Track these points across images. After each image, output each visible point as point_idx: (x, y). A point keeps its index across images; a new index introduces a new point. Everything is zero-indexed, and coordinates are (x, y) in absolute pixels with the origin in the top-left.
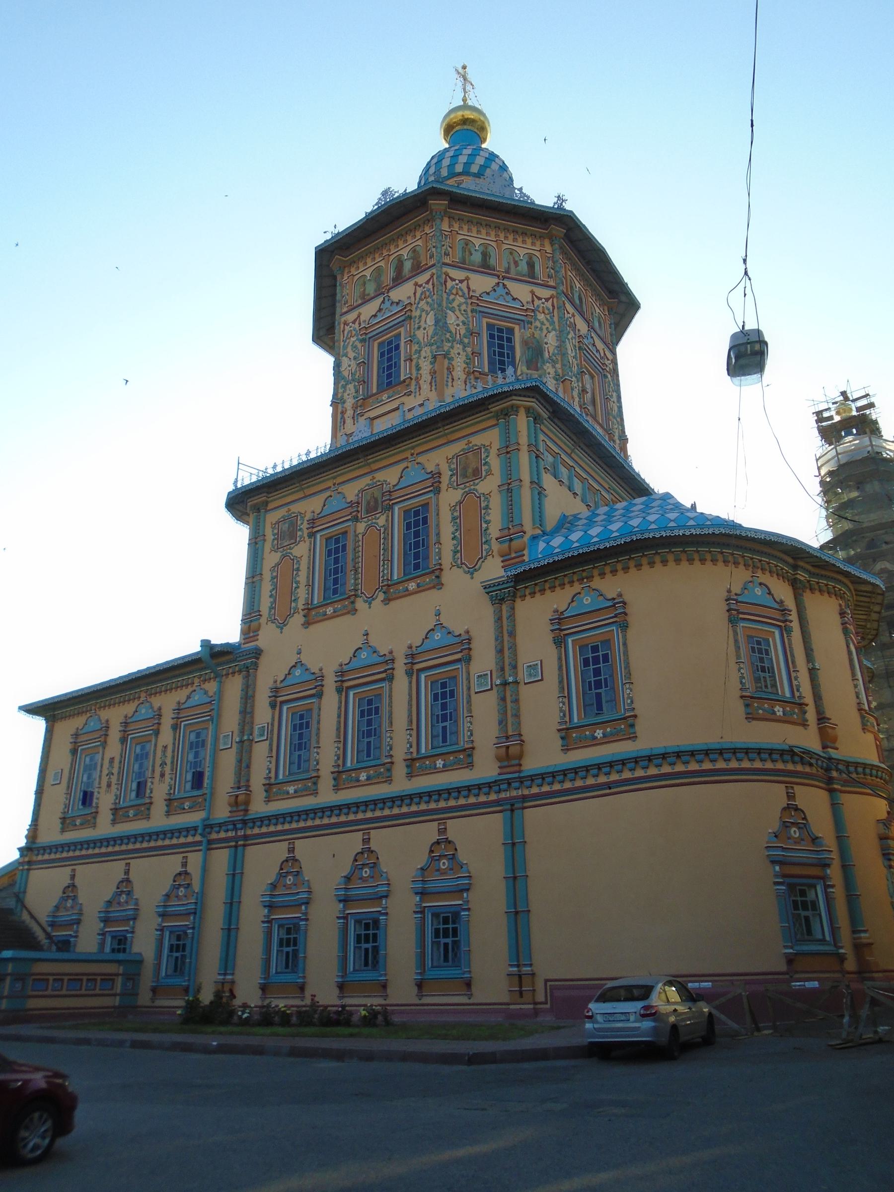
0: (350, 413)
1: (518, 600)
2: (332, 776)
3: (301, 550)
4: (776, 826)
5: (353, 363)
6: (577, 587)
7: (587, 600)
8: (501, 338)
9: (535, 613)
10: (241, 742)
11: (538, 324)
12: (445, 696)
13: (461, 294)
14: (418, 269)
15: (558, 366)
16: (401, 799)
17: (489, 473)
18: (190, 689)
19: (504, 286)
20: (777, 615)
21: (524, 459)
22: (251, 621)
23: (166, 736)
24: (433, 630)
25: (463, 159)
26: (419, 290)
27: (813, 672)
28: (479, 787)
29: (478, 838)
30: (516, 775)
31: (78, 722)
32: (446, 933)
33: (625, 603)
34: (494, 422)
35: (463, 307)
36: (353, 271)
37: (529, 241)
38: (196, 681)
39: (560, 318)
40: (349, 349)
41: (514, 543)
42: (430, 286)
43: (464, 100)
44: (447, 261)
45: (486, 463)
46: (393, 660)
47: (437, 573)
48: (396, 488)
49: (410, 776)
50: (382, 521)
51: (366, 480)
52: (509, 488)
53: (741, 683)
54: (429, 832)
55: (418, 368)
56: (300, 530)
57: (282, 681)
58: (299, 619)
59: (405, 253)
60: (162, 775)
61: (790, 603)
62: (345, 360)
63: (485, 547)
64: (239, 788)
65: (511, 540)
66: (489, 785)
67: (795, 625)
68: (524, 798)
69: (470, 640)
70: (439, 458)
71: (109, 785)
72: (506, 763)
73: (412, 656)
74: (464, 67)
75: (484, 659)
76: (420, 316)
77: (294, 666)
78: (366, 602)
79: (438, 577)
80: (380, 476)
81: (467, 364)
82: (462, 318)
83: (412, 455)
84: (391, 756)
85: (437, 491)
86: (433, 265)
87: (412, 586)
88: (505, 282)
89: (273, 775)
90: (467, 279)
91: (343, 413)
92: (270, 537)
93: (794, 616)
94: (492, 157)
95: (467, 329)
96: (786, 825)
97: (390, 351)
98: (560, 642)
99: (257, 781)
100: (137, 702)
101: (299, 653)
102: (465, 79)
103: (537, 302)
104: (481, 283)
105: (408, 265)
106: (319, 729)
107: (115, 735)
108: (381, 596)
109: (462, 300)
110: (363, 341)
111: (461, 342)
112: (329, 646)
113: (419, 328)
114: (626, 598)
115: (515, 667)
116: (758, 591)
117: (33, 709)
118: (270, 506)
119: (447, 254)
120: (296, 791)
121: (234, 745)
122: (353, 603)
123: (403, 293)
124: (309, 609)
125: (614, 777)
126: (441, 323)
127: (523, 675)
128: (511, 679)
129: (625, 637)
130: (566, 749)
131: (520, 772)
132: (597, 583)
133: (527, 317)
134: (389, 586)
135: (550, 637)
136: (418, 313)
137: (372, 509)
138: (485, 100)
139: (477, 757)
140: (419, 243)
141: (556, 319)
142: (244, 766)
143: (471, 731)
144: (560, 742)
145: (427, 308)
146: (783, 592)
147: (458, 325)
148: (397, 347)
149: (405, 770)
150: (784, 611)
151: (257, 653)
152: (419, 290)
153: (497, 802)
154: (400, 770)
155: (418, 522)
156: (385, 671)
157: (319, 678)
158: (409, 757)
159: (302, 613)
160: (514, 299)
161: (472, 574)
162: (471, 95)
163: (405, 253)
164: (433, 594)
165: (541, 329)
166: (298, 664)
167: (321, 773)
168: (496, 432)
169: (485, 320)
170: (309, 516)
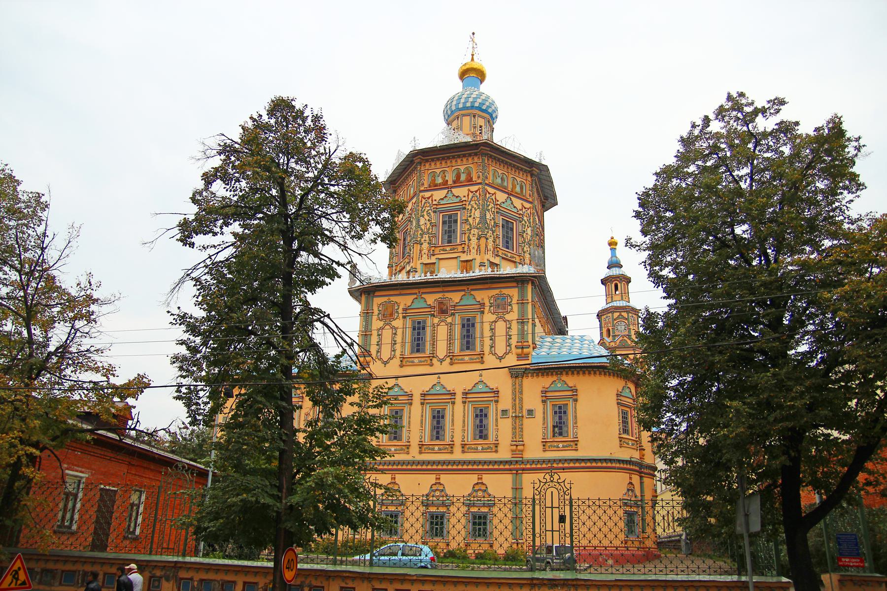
0: (425, 251)
3: (398, 323)
4: (626, 491)
5: (428, 223)
6: (555, 378)
7: (559, 385)
8: (507, 228)
9: (533, 388)
14: (470, 181)
16: (459, 462)
20: (631, 401)
26: (471, 195)
28: (501, 462)
29: (499, 485)
32: (479, 524)
34: (514, 284)
40: (425, 213)
42: (478, 194)
45: (510, 305)
49: (463, 452)
51: (440, 295)
54: (474, 478)
59: (462, 168)
66: (507, 462)
68: (523, 469)
70: (484, 296)
73: (465, 394)
74: (473, 34)
75: (506, 402)
80: (448, 295)
85: (483, 312)
86: (480, 183)
91: (421, 251)
92: (376, 312)
96: (628, 490)
97: (450, 222)
98: (544, 402)
104: (501, 197)
105: (463, 177)
108: (448, 360)
115: (521, 408)
116: (628, 391)
123: (461, 192)
124: (403, 359)
125: (566, 465)
126: (483, 217)
132: (564, 378)
135: (539, 399)
137: (443, 311)
139: (499, 448)
145: (475, 206)
148: (456, 221)
149: (461, 449)
152: (471, 195)
153: (510, 470)
154: (458, 449)
155: (468, 326)
163: (462, 168)
167: (411, 443)
168: (517, 289)
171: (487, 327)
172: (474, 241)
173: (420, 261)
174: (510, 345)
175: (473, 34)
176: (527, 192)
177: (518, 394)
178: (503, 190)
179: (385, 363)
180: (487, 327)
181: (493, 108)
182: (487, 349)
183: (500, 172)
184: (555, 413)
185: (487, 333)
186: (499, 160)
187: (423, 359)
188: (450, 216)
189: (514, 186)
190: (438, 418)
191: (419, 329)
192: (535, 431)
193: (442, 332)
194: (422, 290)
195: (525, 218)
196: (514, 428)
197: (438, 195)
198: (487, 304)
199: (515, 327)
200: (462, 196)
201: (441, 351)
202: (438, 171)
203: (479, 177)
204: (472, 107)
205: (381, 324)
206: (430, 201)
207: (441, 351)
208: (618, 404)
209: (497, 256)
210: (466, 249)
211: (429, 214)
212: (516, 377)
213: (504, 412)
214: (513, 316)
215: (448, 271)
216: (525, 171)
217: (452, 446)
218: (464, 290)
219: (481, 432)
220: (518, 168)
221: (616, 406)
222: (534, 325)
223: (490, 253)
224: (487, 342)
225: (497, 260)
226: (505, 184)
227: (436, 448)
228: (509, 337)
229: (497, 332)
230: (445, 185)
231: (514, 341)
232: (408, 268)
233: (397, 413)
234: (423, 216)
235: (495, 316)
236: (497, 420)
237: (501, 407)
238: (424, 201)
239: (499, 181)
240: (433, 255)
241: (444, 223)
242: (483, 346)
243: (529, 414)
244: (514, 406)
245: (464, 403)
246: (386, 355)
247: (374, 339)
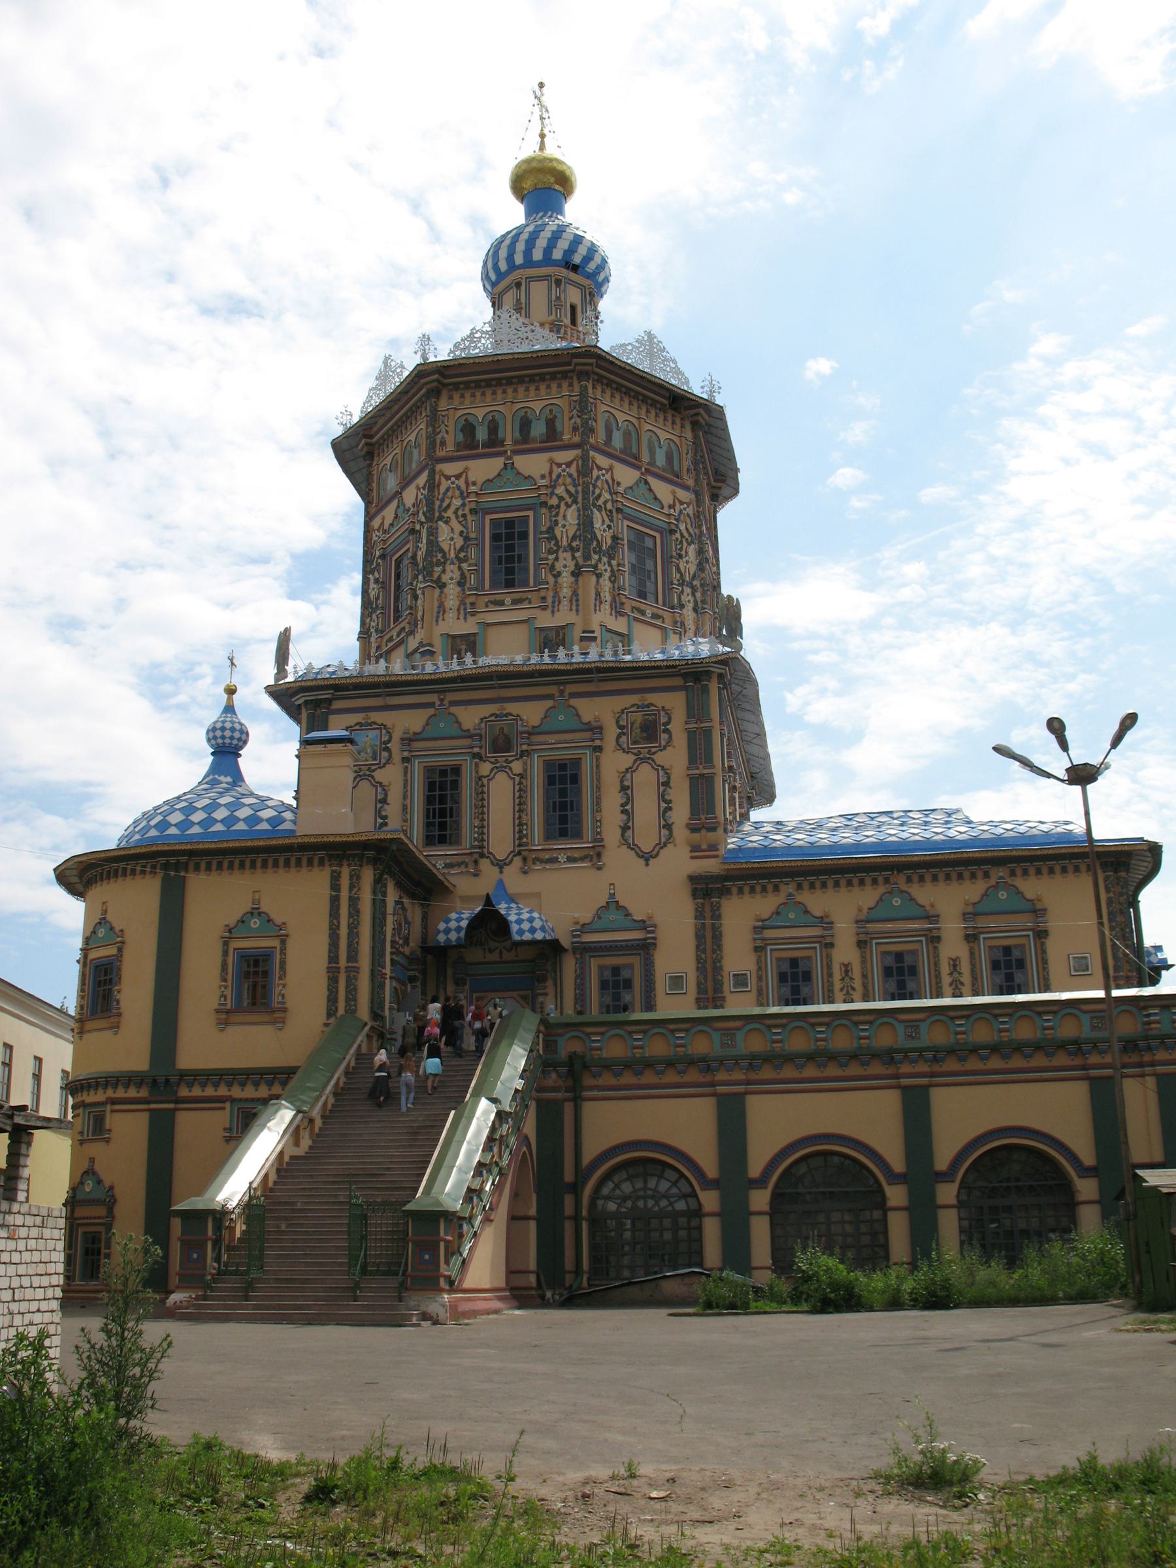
0: (452, 601)
13: (606, 487)
19: (646, 482)
25: (541, 243)
42: (573, 470)
47: (598, 849)
48: (537, 730)
51: (493, 708)
63: (664, 832)
70: (601, 710)
76: (558, 506)
80: (511, 708)
81: (613, 582)
82: (607, 522)
83: (562, 693)
88: (650, 479)
97: (510, 536)
104: (626, 476)
105: (538, 429)
109: (609, 497)
118: (337, 705)
123: (533, 465)
147: (604, 531)
148: (524, 535)
152: (557, 471)
155: (564, 782)
165: (681, 543)
169: (626, 523)
172: (566, 579)
174: (669, 827)
178: (630, 458)
185: (612, 800)
188: (510, 523)
193: (501, 792)
195: (682, 527)
198: (611, 732)
200: (536, 474)
201: (501, 841)
207: (501, 841)
209: (622, 614)
210: (550, 600)
215: (507, 651)
223: (606, 607)
225: (620, 625)
228: (666, 807)
232: (413, 643)
238: (445, 484)
240: (473, 614)
241: (495, 538)
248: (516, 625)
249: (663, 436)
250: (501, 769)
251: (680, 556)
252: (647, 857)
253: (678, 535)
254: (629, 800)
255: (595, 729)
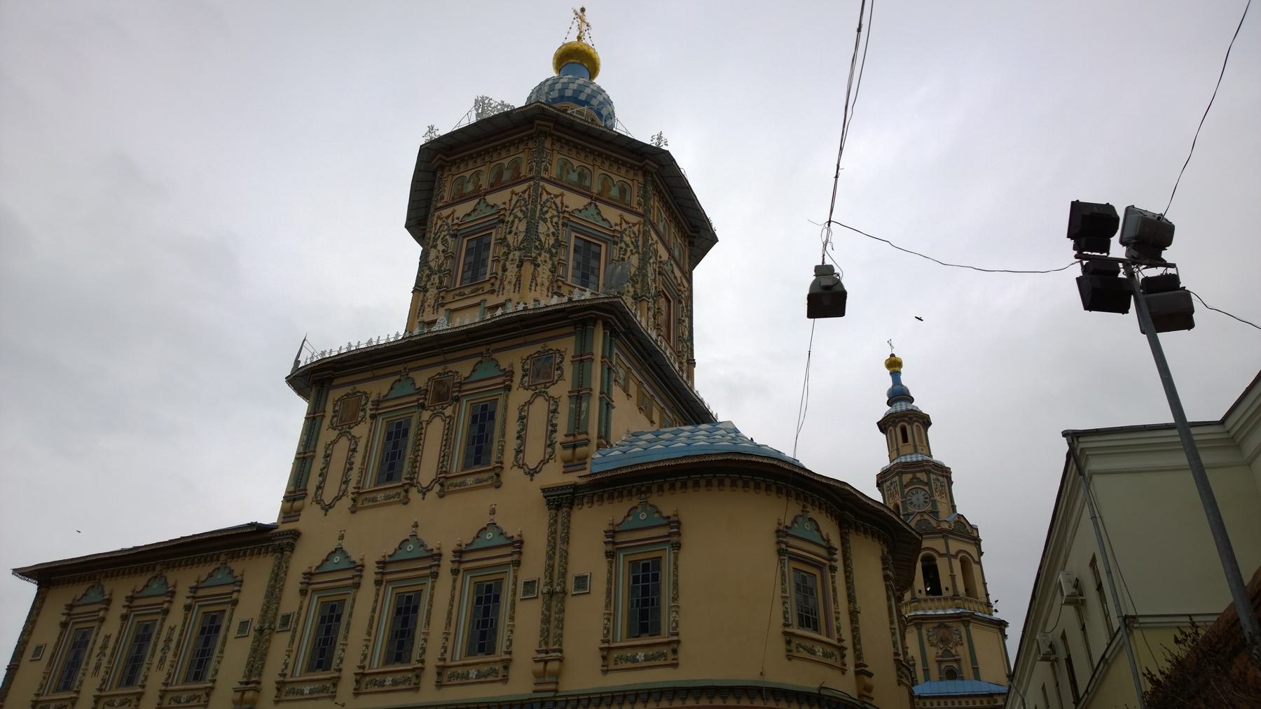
0: (431, 301)
1: (575, 508)
2: (354, 677)
3: (361, 431)
6: (635, 501)
7: (643, 516)
9: (590, 526)
10: (261, 631)
11: (623, 245)
12: (487, 600)
14: (517, 180)
15: (639, 286)
17: (561, 377)
18: (214, 566)
20: (823, 552)
21: (597, 369)
22: (295, 500)
23: (176, 617)
24: (485, 529)
27: (854, 614)
30: (552, 694)
31: (77, 591)
33: (679, 523)
34: (571, 329)
35: (555, 220)
36: (454, 170)
37: (623, 170)
38: (223, 558)
39: (645, 241)
40: (439, 242)
41: (578, 450)
42: (526, 196)
43: (579, 38)
44: (546, 176)
46: (440, 555)
49: (439, 685)
50: (448, 411)
51: (439, 369)
52: (579, 395)
53: (785, 618)
55: (504, 270)
56: (363, 410)
57: (318, 568)
58: (346, 502)
60: (162, 661)
61: (836, 542)
62: (433, 253)
63: (549, 450)
64: (247, 683)
65: (575, 447)
67: (839, 564)
69: (522, 542)
70: (514, 359)
71: (97, 667)
72: (541, 680)
73: (459, 553)
74: (583, 10)
75: (534, 566)
77: (334, 552)
78: (419, 492)
79: (498, 475)
80: (452, 367)
82: (552, 230)
84: (422, 661)
85: (509, 388)
86: (532, 178)
87: (470, 481)
89: (288, 672)
90: (562, 195)
91: (423, 302)
93: (839, 556)
94: (600, 91)
95: (557, 240)
98: (610, 555)
99: (270, 679)
100: (149, 575)
101: (342, 538)
102: (583, 21)
103: (624, 225)
104: (574, 201)
105: (507, 176)
106: (349, 624)
107: (117, 609)
108: (437, 488)
110: (454, 236)
111: (549, 251)
112: (374, 534)
113: (510, 232)
114: (683, 521)
115: (563, 575)
117: (25, 573)
118: (336, 382)
119: (546, 170)
120: (311, 692)
121: (252, 633)
122: (406, 491)
123: (499, 198)
124: (358, 493)
126: (531, 230)
127: (570, 585)
128: (558, 589)
129: (676, 558)
130: (605, 672)
131: (556, 691)
132: (654, 499)
133: (614, 238)
134: (447, 478)
136: (511, 218)
138: (598, 43)
139: (513, 673)
140: (521, 155)
141: (640, 243)
142: (258, 657)
143: (511, 641)
144: (600, 662)
145: (520, 215)
146: (829, 529)
150: (831, 550)
151: (296, 535)
152: (515, 198)
154: (429, 677)
155: (483, 420)
156: (431, 567)
157: (359, 568)
158: (442, 663)
159: (351, 496)
160: (604, 220)
161: (532, 475)
162: (587, 36)
163: (506, 162)
164: (492, 492)
166: (339, 550)
169: (573, 234)
170: (373, 397)
171: (513, 415)
172: (512, 269)
173: (421, 319)
175: (583, 10)
176: (634, 199)
177: (559, 542)
179: (327, 508)
180: (513, 415)
181: (600, 98)
182: (509, 457)
183: (576, 164)
184: (636, 580)
185: (513, 427)
186: (575, 146)
187: (392, 493)
189: (606, 188)
190: (407, 611)
191: (397, 436)
192: (588, 620)
193: (435, 432)
194: (411, 365)
195: (627, 239)
196: (546, 620)
197: (462, 209)
198: (518, 373)
199: (565, 408)
200: (499, 203)
202: (468, 174)
203: (531, 170)
204: (562, 98)
205: (333, 434)
206: (450, 221)
208: (781, 552)
210: (496, 287)
211: (444, 241)
212: (558, 507)
213: (530, 585)
214: (562, 389)
216: (632, 167)
217: (419, 672)
218: (481, 354)
219: (483, 634)
220: (616, 161)
221: (775, 558)
222: (607, 405)
224: (512, 443)
226: (587, 183)
227: (389, 680)
229: (531, 421)
230: (479, 194)
231: (560, 437)
233: (333, 608)
234: (435, 247)
235: (530, 393)
236: (513, 605)
237: (525, 574)
239: (574, 177)
240: (443, 305)
241: (468, 252)
242: (502, 451)
243: (578, 587)
244: (550, 569)
245: (455, 572)
246: (329, 493)
247: (317, 465)
248: (470, 311)
249: (616, 178)
250: (435, 415)
251: (623, 259)
252: (532, 473)
253: (623, 245)
254: (524, 427)
255: (510, 374)
